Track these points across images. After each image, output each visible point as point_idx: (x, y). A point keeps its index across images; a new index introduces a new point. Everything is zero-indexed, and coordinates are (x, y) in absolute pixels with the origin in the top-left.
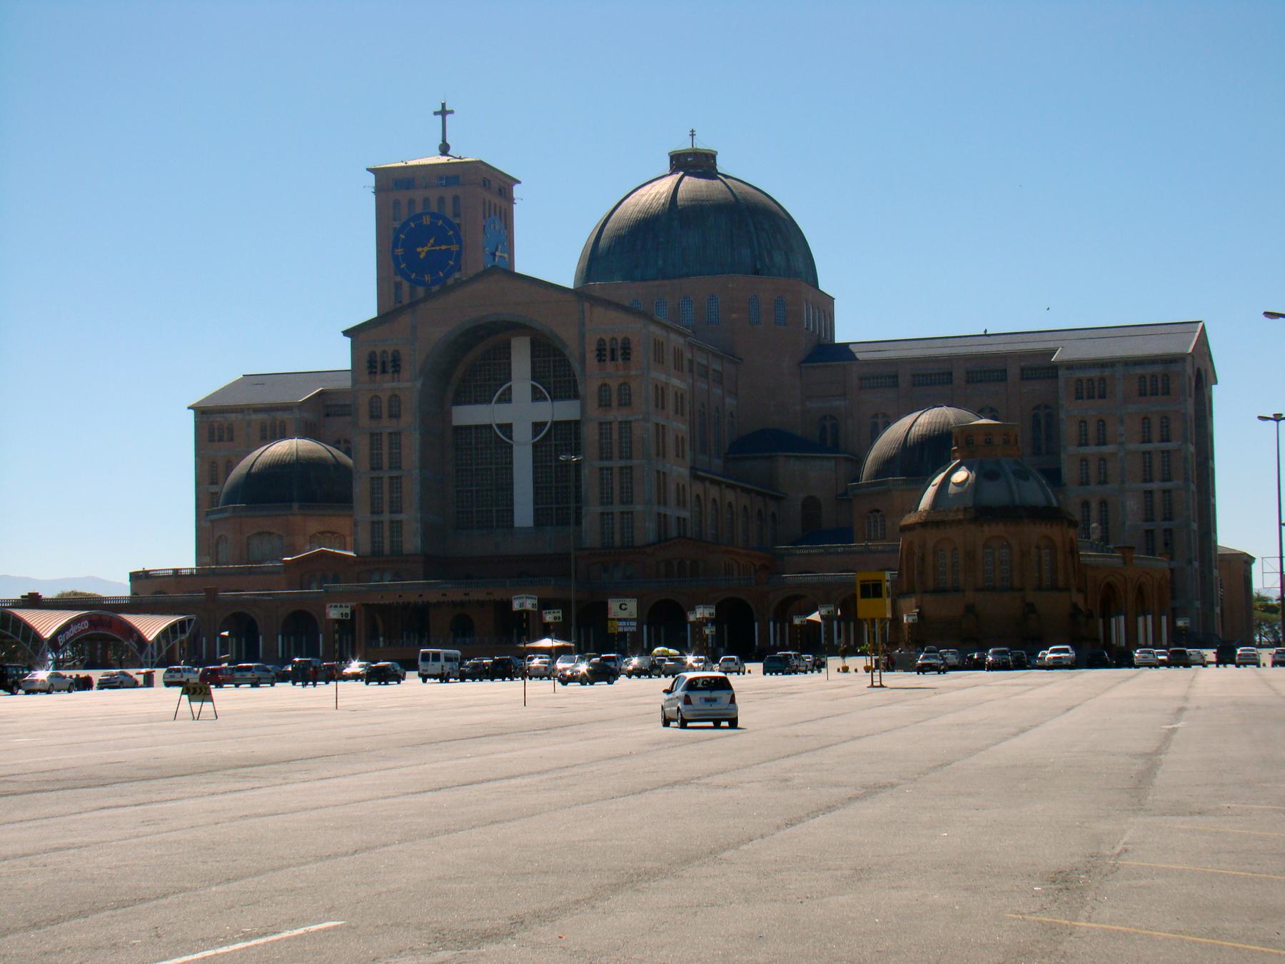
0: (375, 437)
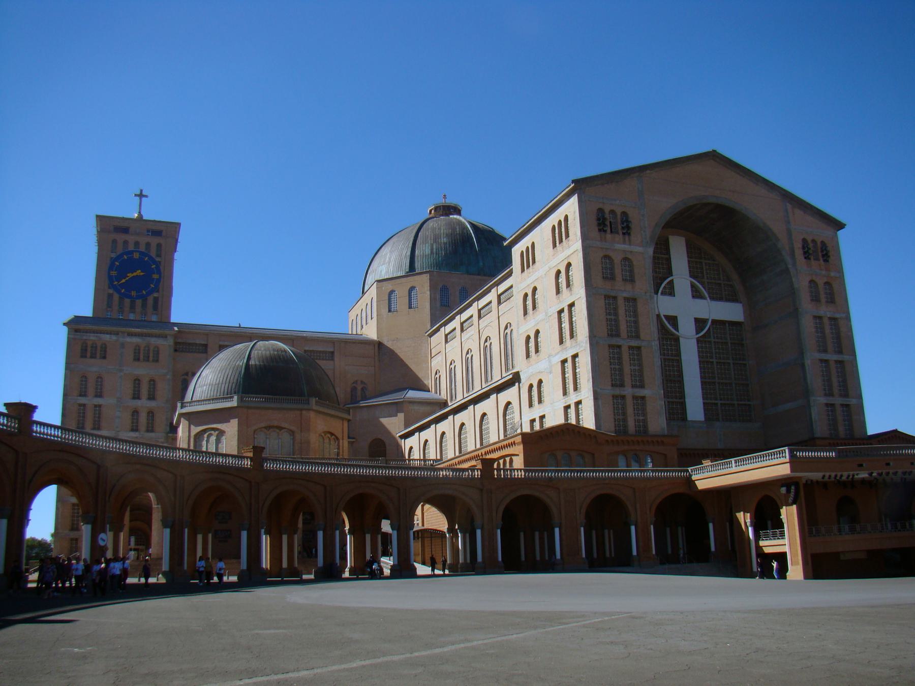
0: (611, 299)
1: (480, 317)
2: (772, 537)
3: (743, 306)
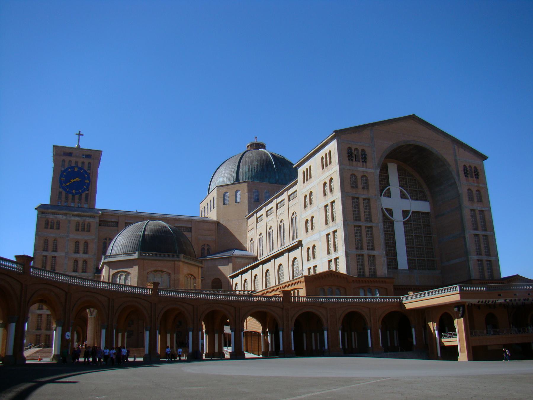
0: (355, 199)
1: (277, 208)
2: (449, 336)
3: (430, 203)
